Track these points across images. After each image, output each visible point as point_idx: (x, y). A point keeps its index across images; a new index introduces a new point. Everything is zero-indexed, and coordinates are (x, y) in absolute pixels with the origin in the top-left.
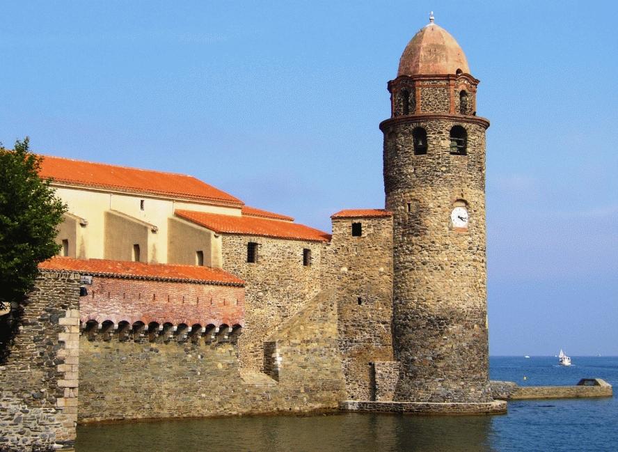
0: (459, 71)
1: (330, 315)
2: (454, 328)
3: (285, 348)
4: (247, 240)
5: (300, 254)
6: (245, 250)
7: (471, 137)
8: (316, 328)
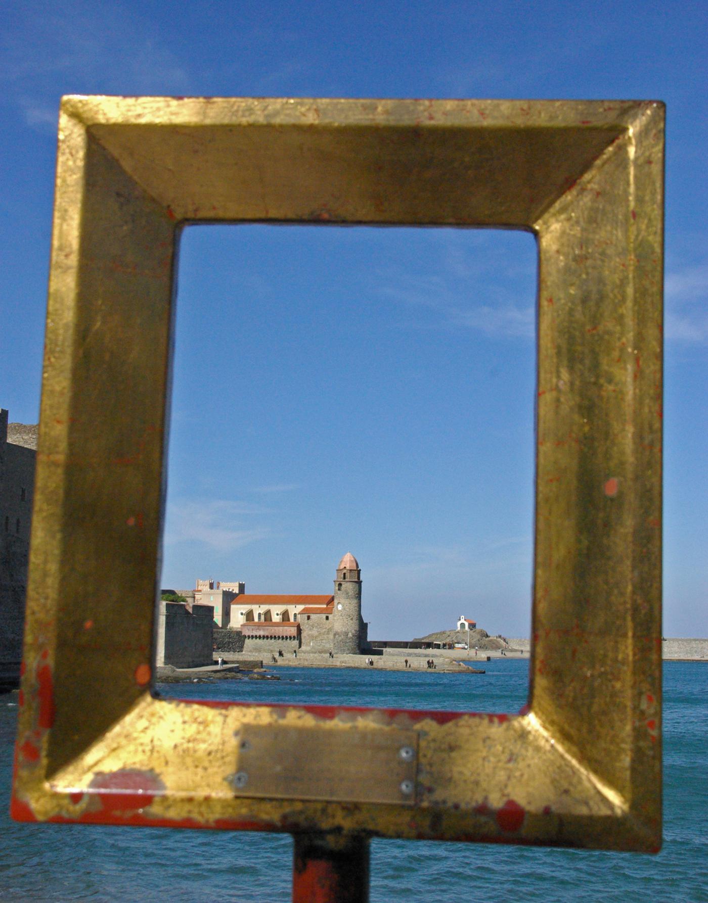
0: (345, 567)
1: (330, 633)
2: (337, 636)
3: (314, 641)
4: (307, 615)
5: (325, 617)
6: (306, 618)
7: (343, 585)
8: (325, 636)
